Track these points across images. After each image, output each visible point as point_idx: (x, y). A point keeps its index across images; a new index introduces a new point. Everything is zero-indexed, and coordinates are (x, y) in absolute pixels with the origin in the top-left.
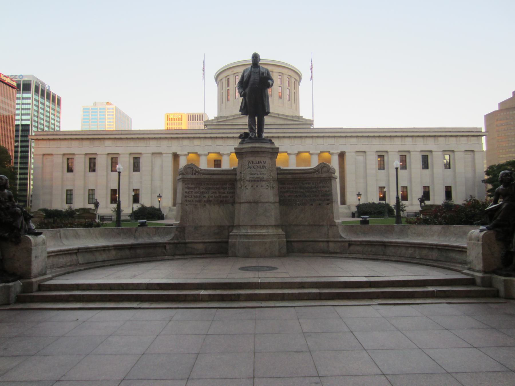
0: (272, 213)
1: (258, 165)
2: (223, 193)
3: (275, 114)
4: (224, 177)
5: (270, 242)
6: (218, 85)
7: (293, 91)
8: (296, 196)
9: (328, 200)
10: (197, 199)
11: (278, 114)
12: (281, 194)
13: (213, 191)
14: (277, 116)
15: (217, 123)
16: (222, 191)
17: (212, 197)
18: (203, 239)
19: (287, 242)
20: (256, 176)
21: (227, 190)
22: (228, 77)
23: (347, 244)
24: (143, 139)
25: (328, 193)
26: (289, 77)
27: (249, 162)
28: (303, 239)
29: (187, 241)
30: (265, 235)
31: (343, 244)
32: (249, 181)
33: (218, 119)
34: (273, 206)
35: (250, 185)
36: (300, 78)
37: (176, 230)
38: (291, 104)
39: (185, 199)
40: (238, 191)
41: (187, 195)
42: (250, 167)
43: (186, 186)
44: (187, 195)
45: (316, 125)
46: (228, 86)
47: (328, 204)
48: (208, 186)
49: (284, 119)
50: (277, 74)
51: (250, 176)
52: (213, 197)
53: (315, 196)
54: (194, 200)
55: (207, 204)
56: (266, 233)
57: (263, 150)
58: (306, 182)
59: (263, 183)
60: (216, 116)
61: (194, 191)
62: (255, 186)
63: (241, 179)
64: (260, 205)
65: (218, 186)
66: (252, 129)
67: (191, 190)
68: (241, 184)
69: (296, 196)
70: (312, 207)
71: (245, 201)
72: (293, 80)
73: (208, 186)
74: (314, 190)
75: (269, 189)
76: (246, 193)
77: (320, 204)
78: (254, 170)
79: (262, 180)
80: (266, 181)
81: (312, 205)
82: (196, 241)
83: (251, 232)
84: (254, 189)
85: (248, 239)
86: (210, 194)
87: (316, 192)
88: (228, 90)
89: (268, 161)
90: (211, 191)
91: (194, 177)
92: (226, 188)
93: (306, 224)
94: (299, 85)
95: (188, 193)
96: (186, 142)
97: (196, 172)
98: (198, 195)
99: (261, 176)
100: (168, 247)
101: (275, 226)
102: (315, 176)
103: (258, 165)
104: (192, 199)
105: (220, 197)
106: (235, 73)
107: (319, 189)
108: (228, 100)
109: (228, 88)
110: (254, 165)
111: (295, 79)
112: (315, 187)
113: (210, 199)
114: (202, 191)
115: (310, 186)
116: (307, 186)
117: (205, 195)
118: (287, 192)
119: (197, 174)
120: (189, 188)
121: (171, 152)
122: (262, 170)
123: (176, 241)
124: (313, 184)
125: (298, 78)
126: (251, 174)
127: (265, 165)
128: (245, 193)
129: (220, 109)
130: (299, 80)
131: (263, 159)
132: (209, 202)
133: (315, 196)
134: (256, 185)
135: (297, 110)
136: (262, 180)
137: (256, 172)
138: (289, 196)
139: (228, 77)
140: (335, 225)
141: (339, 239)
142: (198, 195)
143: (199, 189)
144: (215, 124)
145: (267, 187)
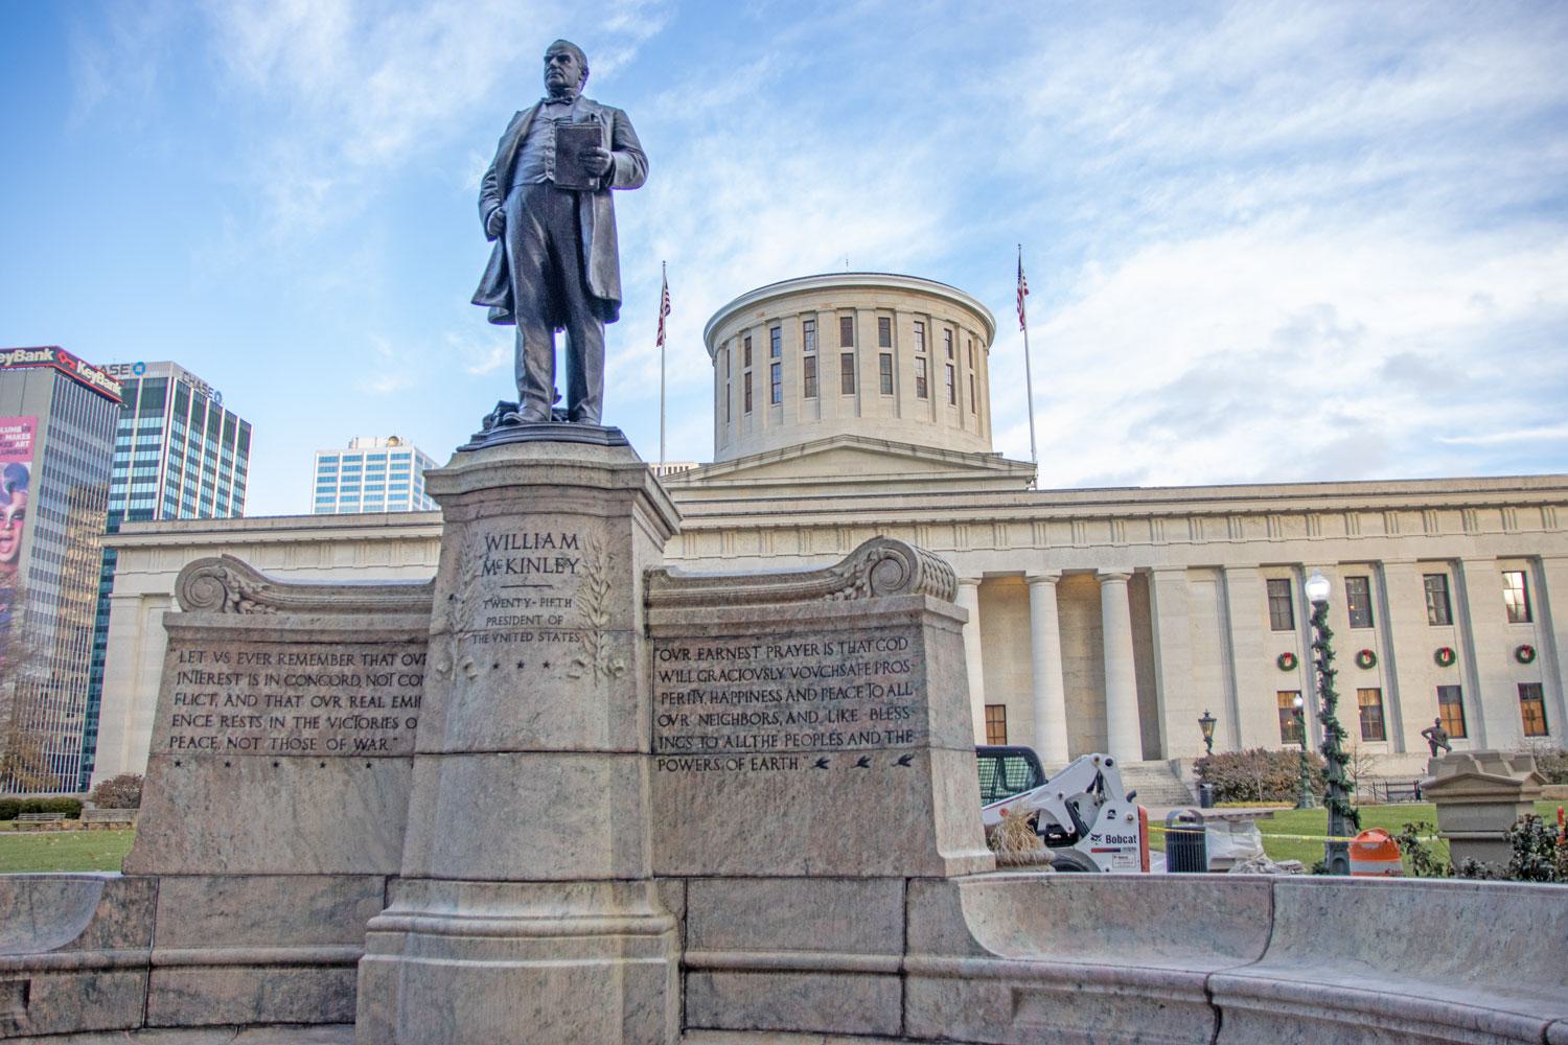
0: (601, 815)
1: (533, 555)
2: (375, 702)
3: (901, 445)
4: (381, 623)
5: (570, 972)
6: (714, 362)
7: (966, 372)
8: (743, 719)
9: (906, 736)
10: (237, 733)
11: (913, 448)
12: (666, 706)
13: (324, 691)
14: (909, 453)
15: (705, 484)
16: (368, 691)
17: (314, 722)
18: (250, 943)
19: (686, 969)
20: (519, 611)
21: (394, 689)
22: (746, 336)
23: (1004, 989)
25: (907, 701)
26: (950, 327)
27: (492, 543)
28: (774, 957)
29: (158, 954)
30: (540, 935)
31: (982, 989)
32: (485, 640)
33: (706, 471)
34: (604, 770)
35: (489, 660)
37: (106, 896)
39: (176, 732)
40: (431, 690)
41: (184, 710)
42: (496, 566)
43: (187, 667)
44: (184, 710)
45: (1047, 480)
46: (748, 363)
47: (904, 761)
48: (300, 670)
49: (933, 462)
50: (910, 319)
51: (492, 612)
52: (322, 723)
53: (842, 715)
54: (223, 739)
55: (284, 761)
56: (550, 925)
57: (559, 476)
58: (792, 642)
59: (556, 651)
60: (710, 459)
61: (223, 697)
62: (513, 667)
63: (447, 632)
64: (528, 762)
65: (348, 670)
66: (528, 381)
67: (210, 689)
68: (449, 658)
69: (743, 719)
70: (823, 775)
71: (461, 745)
72: (964, 337)
73: (300, 670)
74: (834, 682)
75: (588, 679)
76: (464, 703)
77: (862, 763)
78: (511, 579)
79: (550, 632)
80: (575, 634)
81: (821, 764)
82: (205, 953)
83: (471, 914)
84: (506, 679)
85: (453, 955)
86: (306, 710)
87: (843, 693)
88: (748, 375)
89: (590, 532)
90: (313, 689)
91: (231, 620)
92: (388, 678)
93: (791, 870)
95: (195, 700)
97: (244, 597)
98: (246, 711)
99: (546, 612)
100: (40, 986)
101: (613, 880)
102: (839, 606)
103: (533, 555)
104: (212, 732)
105: (358, 726)
106: (768, 322)
107: (861, 681)
108: (748, 408)
109: (747, 370)
110: (512, 554)
111: (970, 332)
112: (840, 670)
113: (307, 733)
114: (266, 690)
115: (812, 661)
116: (797, 662)
117: (278, 713)
118: (696, 695)
119: (246, 605)
120: (200, 678)
122: (554, 579)
123: (93, 956)
124: (829, 652)
125: (981, 331)
126: (496, 603)
127: (572, 554)
128: (462, 705)
129: (721, 440)
130: (984, 336)
131: (557, 527)
132: (300, 750)
133: (842, 715)
134: (516, 659)
136: (550, 632)
137: (523, 594)
138: (707, 720)
139: (746, 336)
140: (943, 880)
141: (963, 962)
142: (246, 711)
143: (254, 681)
144: (698, 484)
145: (578, 672)
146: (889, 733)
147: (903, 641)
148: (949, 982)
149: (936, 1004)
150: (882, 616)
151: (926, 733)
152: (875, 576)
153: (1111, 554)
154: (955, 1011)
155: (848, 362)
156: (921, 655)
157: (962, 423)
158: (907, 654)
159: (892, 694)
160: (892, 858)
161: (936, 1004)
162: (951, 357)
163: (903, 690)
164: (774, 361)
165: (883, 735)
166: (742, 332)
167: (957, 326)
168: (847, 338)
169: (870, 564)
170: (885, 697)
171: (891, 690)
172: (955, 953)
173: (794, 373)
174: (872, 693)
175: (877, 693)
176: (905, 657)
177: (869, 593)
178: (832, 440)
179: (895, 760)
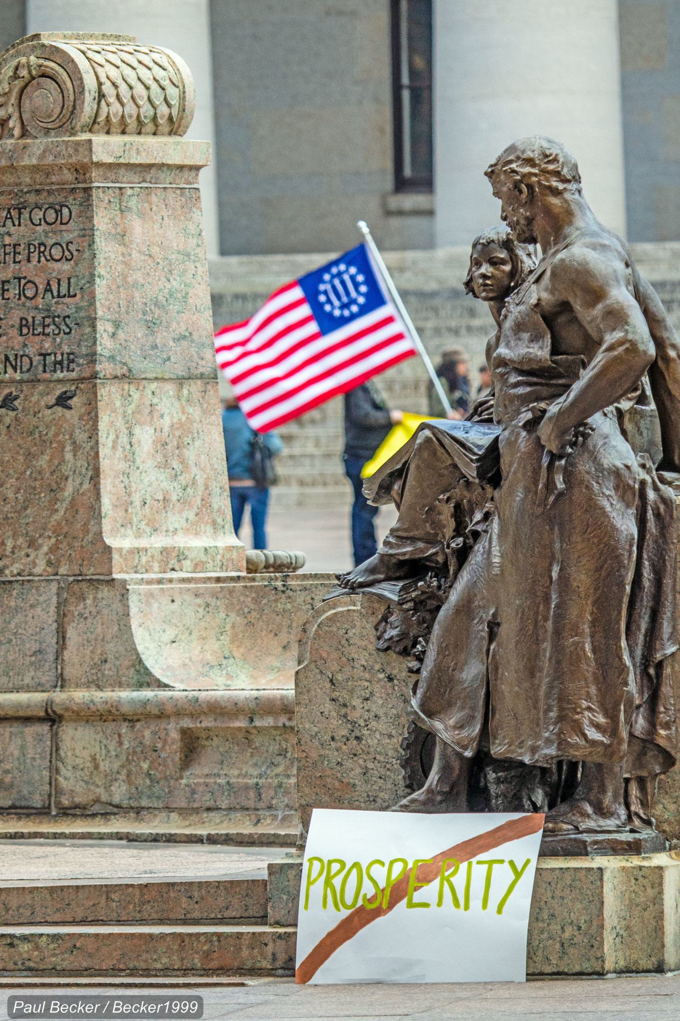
146: (44, 355)
147: (65, 211)
148: (111, 727)
149: (94, 759)
150: (35, 169)
151: (92, 358)
152: (27, 105)
154: (116, 766)
156: (88, 233)
158: (70, 233)
159: (49, 295)
160: (45, 549)
161: (94, 759)
163: (64, 291)
165: (37, 359)
169: (18, 84)
170: (39, 300)
171: (48, 289)
172: (120, 685)
174: (22, 294)
175: (30, 293)
176: (68, 237)
177: (17, 132)
179: (52, 400)
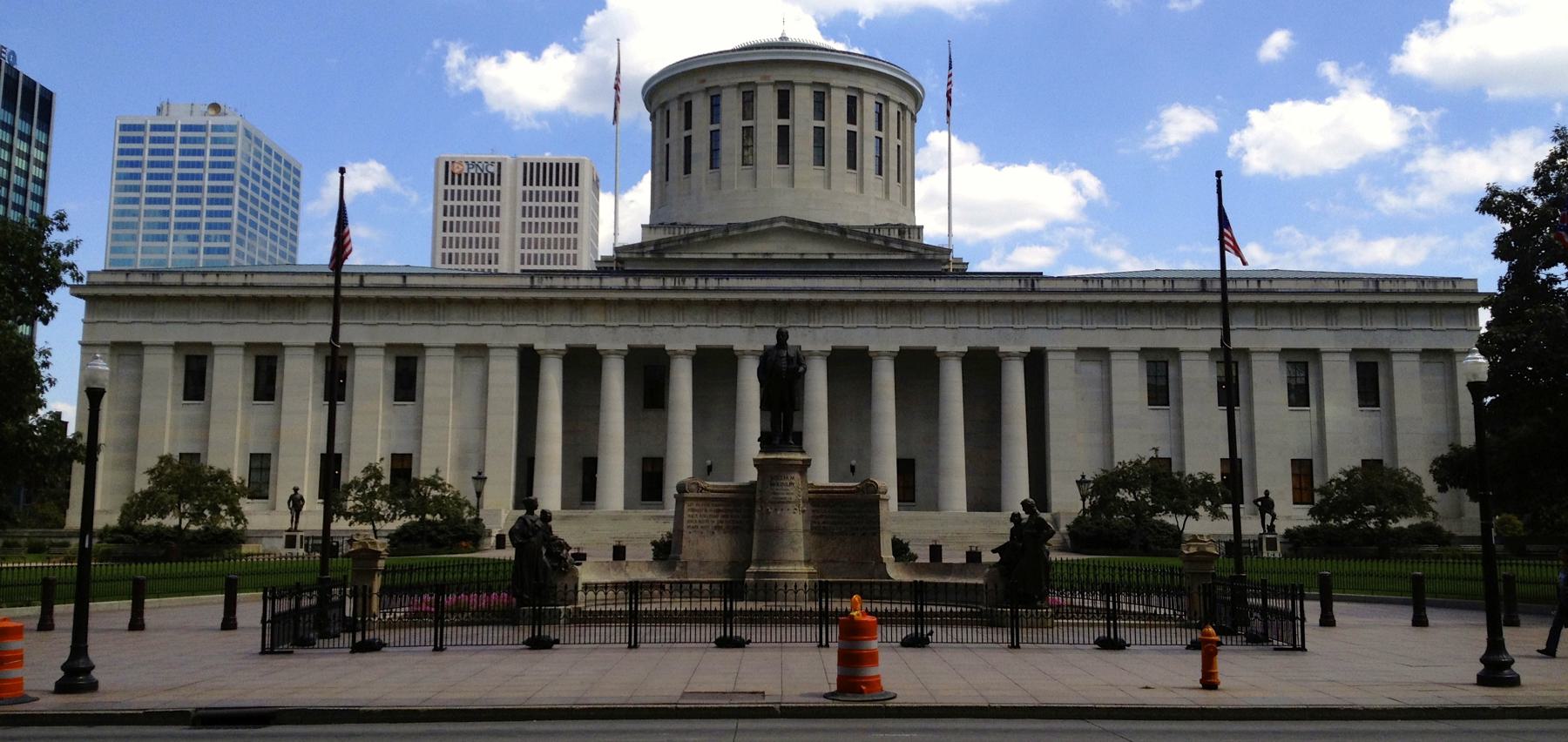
6: (653, 118)
7: (894, 142)
24: (432, 302)
36: (918, 100)
38: (887, 185)
46: (688, 126)
94: (914, 119)
96: (560, 317)
109: (687, 133)
121: (516, 343)
125: (909, 102)
130: (911, 106)
135: (904, 203)
153: (1013, 340)
155: (784, 134)
157: (887, 193)
162: (880, 129)
164: (714, 127)
166: (681, 97)
167: (886, 99)
168: (784, 110)
173: (731, 142)
178: (773, 221)
